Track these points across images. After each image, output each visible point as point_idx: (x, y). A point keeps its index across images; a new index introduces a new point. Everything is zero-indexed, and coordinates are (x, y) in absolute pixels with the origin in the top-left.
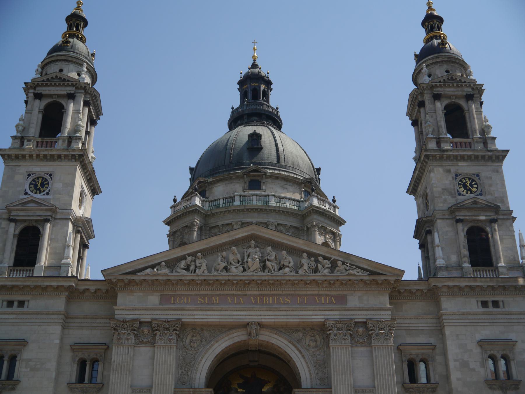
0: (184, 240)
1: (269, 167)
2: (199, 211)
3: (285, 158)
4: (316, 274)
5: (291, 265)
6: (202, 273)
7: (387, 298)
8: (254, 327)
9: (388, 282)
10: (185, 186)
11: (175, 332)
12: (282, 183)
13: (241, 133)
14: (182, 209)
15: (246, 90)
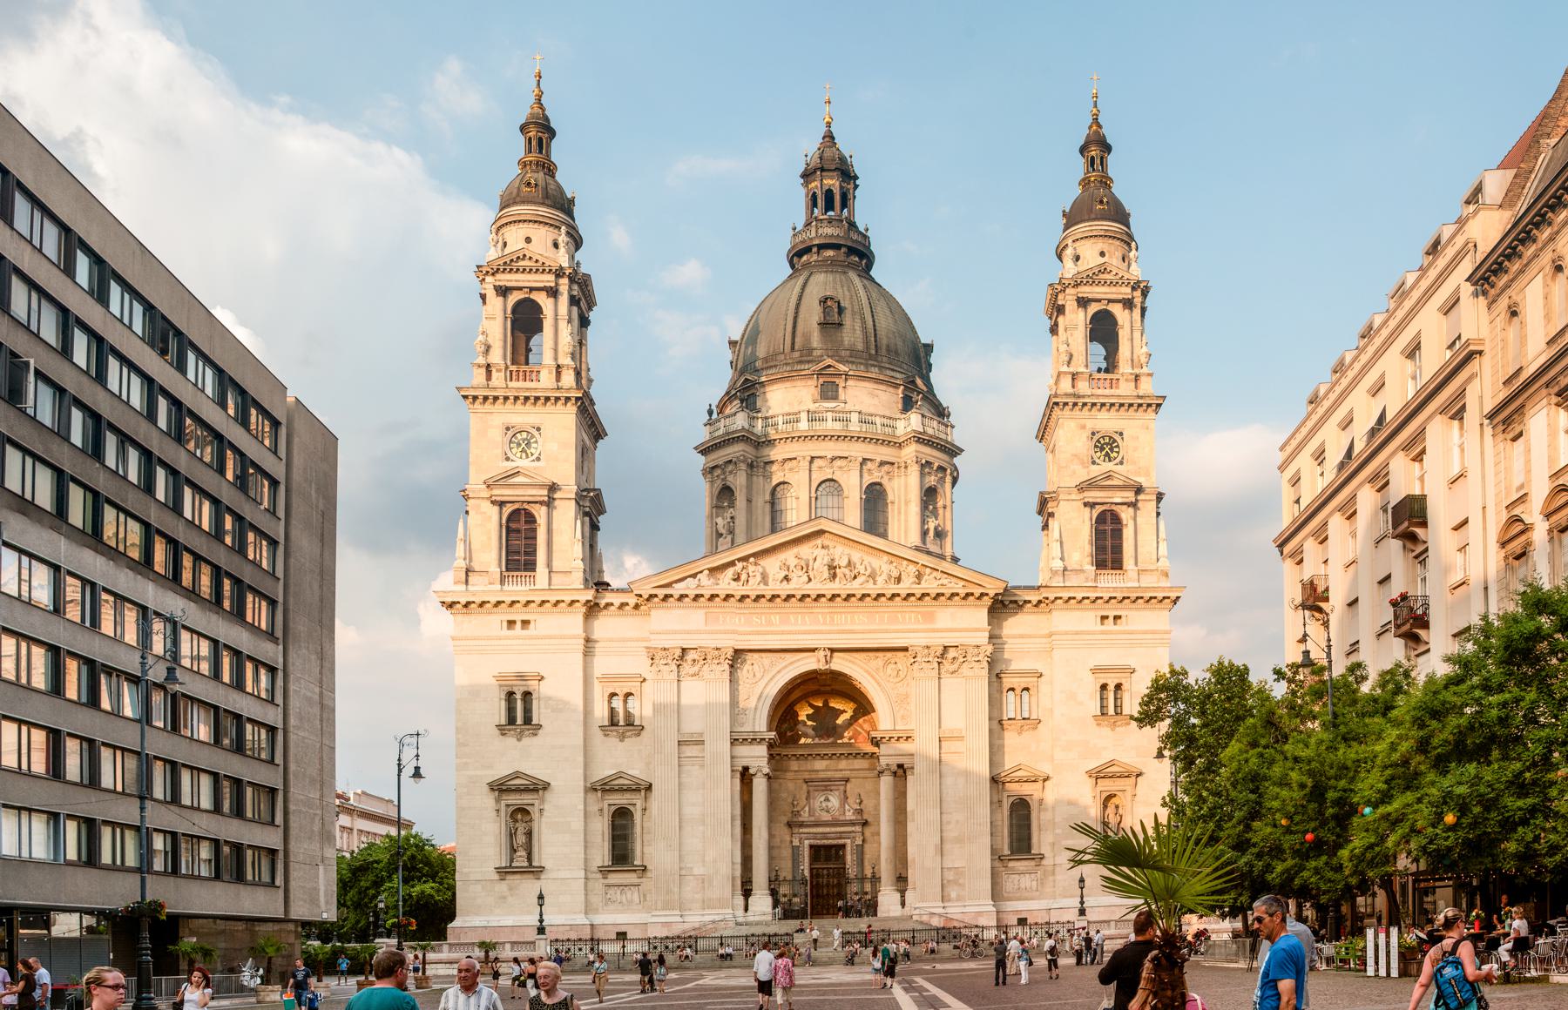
0: (728, 483)
1: (853, 359)
2: (748, 438)
3: (876, 341)
4: (900, 586)
5: (867, 573)
6: (753, 588)
7: (983, 614)
8: (822, 653)
9: (987, 594)
10: (721, 379)
11: (727, 661)
12: (870, 385)
13: (807, 290)
14: (721, 432)
15: (815, 193)
